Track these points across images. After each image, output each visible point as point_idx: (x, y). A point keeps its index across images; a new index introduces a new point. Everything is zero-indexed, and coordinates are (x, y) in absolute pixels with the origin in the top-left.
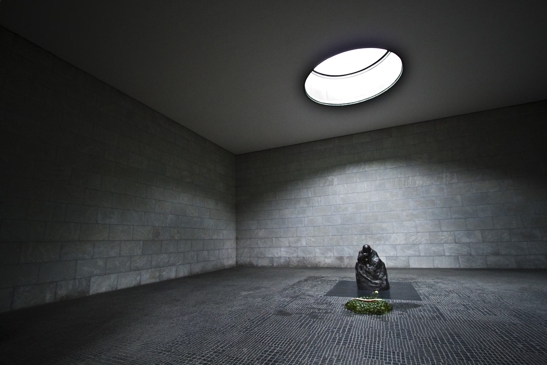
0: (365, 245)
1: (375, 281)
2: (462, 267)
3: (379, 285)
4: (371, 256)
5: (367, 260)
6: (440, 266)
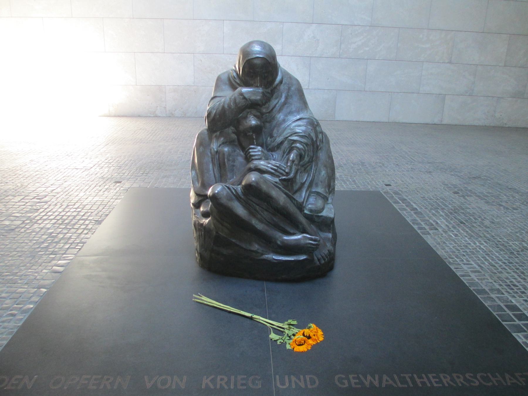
0: (250, 44)
1: (286, 238)
2: (445, 122)
3: (303, 257)
4: (273, 102)
6: (401, 119)
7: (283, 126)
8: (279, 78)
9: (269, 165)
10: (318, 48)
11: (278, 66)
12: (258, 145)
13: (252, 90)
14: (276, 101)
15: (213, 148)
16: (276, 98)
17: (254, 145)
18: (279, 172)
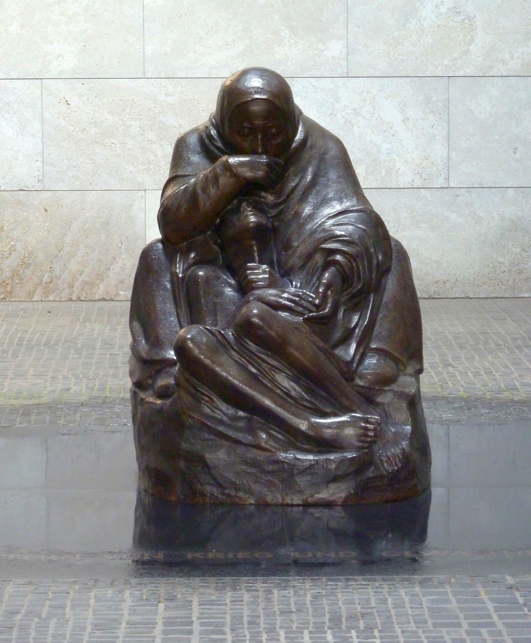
5: (252, 219)
7: (309, 226)
8: (299, 136)
9: (285, 295)
10: (473, 44)
11: (297, 112)
12: (261, 262)
13: (247, 159)
14: (297, 181)
15: (176, 272)
16: (296, 175)
17: (254, 262)
18: (302, 306)
